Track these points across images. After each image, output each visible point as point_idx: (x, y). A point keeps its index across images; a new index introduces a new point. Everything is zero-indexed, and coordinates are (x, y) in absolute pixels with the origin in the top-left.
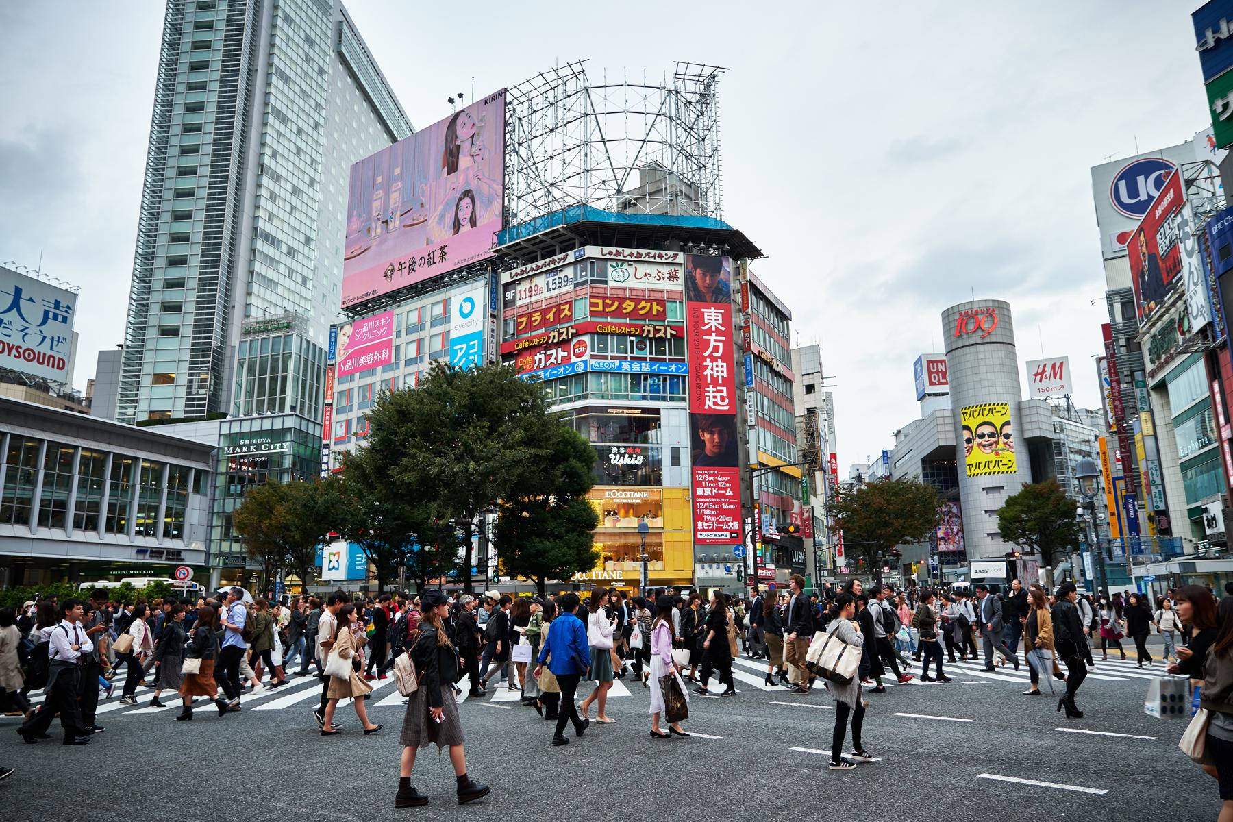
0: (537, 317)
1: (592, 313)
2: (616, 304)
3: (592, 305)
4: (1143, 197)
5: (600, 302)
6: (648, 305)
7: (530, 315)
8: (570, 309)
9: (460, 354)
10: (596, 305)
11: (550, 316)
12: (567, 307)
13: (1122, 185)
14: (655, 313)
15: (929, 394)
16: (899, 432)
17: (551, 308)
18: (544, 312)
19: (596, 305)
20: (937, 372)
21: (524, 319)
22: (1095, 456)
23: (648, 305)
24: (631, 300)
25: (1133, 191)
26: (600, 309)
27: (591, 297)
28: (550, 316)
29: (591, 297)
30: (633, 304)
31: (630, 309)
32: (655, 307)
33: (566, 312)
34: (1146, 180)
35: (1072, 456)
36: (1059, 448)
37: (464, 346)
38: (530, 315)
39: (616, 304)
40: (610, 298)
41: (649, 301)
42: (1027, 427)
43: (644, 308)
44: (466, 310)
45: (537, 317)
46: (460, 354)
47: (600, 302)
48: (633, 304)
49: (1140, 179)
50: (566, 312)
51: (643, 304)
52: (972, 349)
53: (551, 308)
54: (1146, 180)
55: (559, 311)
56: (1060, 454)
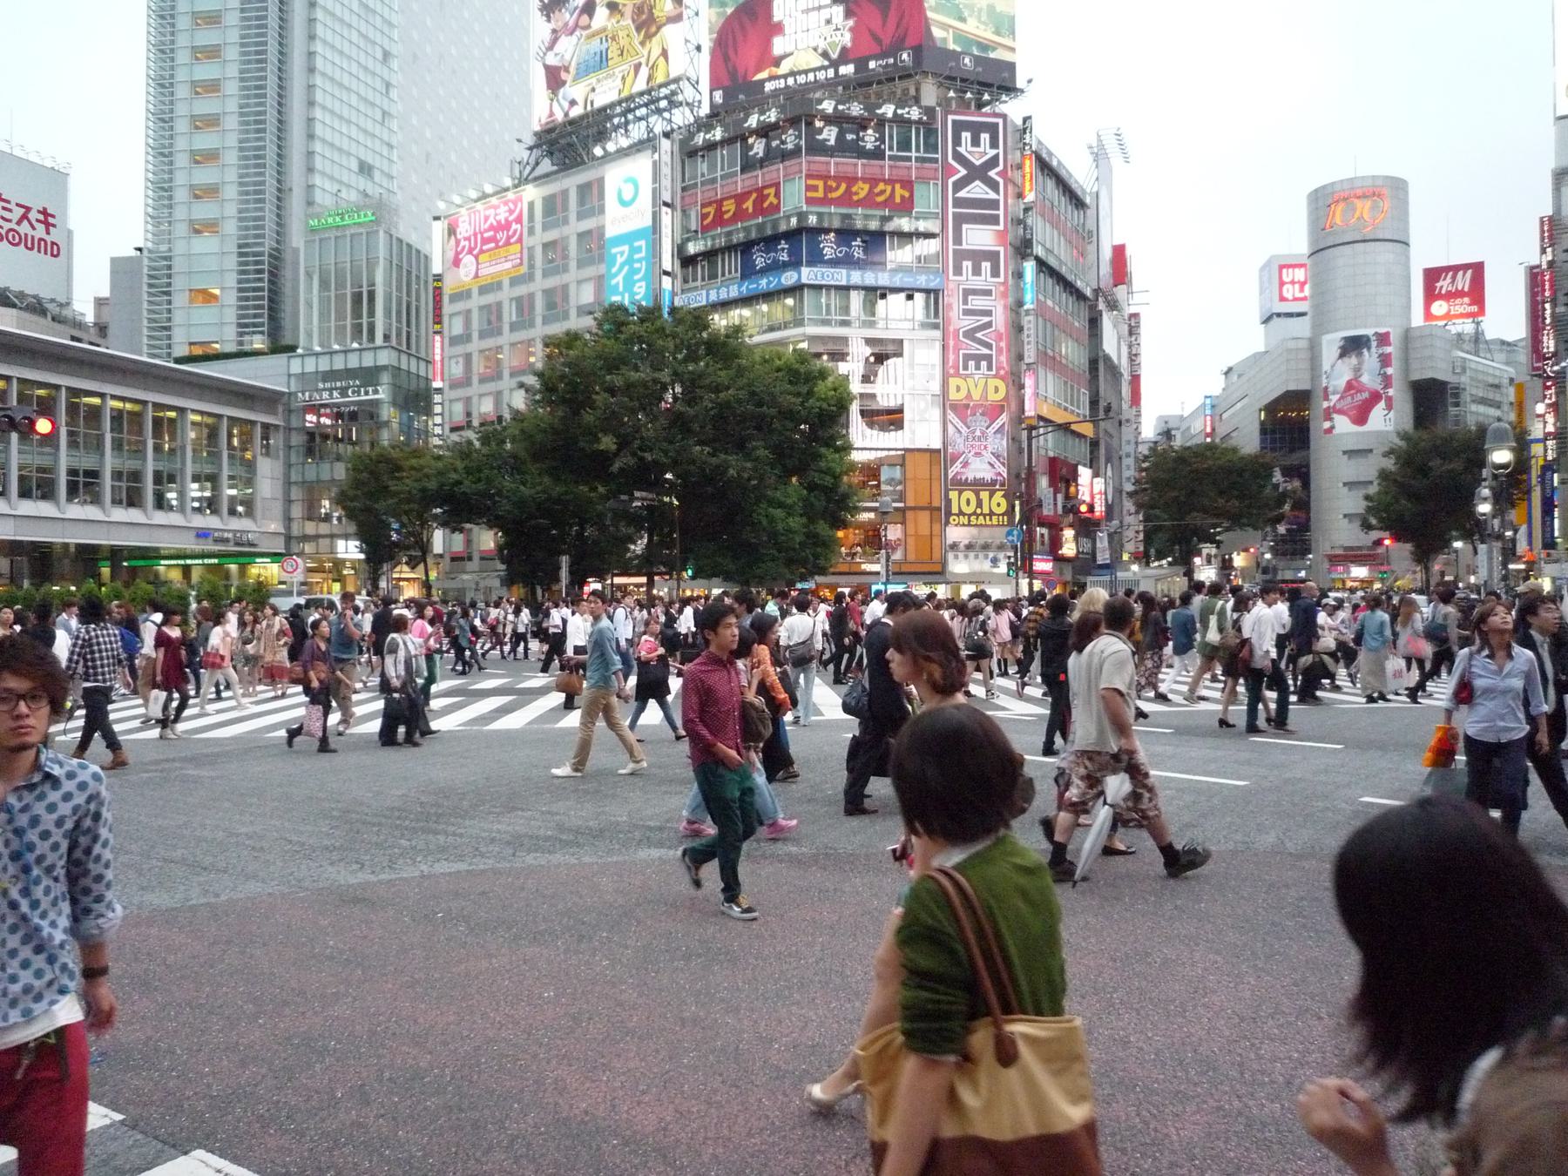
0: (729, 206)
1: (809, 201)
2: (843, 186)
3: (809, 188)
5: (820, 184)
6: (889, 188)
7: (720, 203)
8: (777, 195)
9: (620, 260)
10: (815, 188)
11: (749, 205)
12: (772, 191)
14: (898, 200)
15: (1279, 315)
16: (1230, 369)
17: (750, 193)
18: (740, 198)
19: (815, 188)
20: (1293, 282)
21: (711, 210)
22: (1506, 408)
23: (889, 188)
24: (864, 180)
26: (820, 194)
27: (809, 176)
28: (749, 205)
29: (809, 176)
30: (866, 187)
31: (862, 194)
32: (899, 191)
33: (772, 199)
35: (1474, 408)
36: (1456, 395)
37: (626, 248)
38: (720, 203)
39: (843, 186)
40: (835, 178)
41: (891, 182)
42: (1414, 365)
43: (882, 192)
44: (627, 196)
45: (729, 206)
46: (620, 260)
47: (820, 184)
48: (866, 187)
51: (881, 186)
52: (1347, 249)
53: (750, 193)
55: (762, 198)
56: (1457, 405)
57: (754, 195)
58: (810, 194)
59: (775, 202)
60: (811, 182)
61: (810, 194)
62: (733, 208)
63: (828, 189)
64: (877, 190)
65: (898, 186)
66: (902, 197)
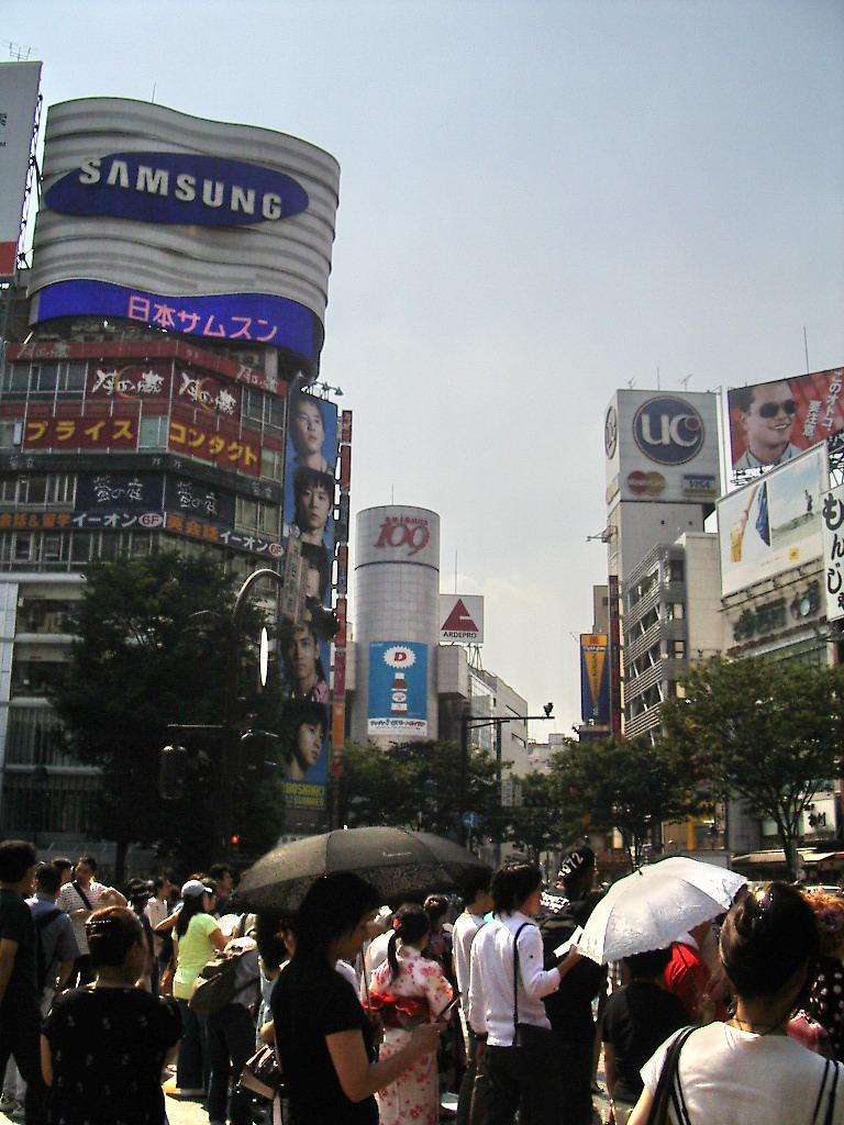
1: (172, 444)
4: (665, 440)
8: (133, 429)
10: (177, 433)
11: (94, 432)
12: (126, 424)
13: (646, 419)
14: (247, 462)
19: (177, 433)
21: (41, 427)
25: (656, 431)
26: (181, 440)
28: (94, 432)
33: (124, 432)
34: (670, 420)
43: (236, 451)
49: (665, 419)
50: (124, 432)
54: (670, 420)
57: (102, 424)
58: (173, 438)
59: (129, 436)
60: (175, 426)
61: (173, 438)
62: (71, 431)
63: (191, 437)
64: (230, 449)
65: (248, 449)
66: (252, 461)
